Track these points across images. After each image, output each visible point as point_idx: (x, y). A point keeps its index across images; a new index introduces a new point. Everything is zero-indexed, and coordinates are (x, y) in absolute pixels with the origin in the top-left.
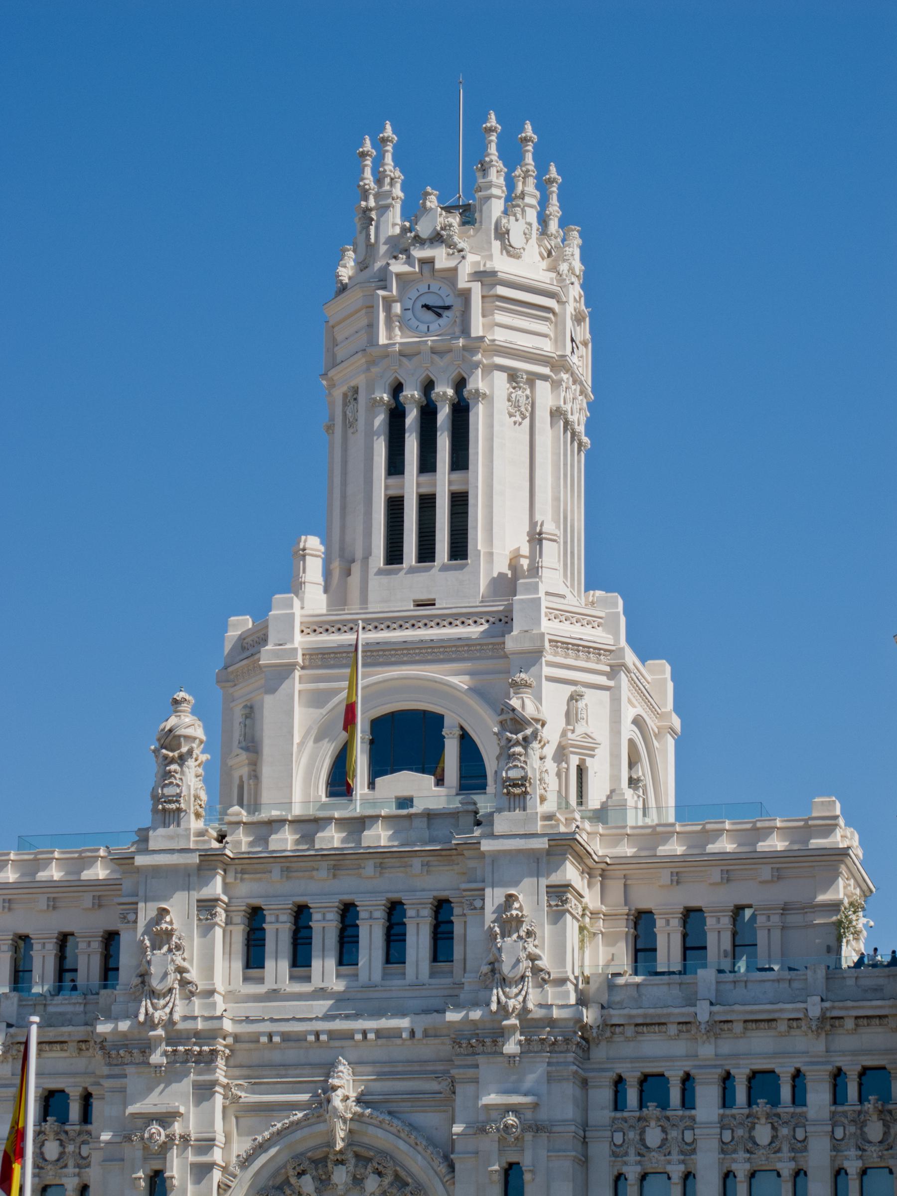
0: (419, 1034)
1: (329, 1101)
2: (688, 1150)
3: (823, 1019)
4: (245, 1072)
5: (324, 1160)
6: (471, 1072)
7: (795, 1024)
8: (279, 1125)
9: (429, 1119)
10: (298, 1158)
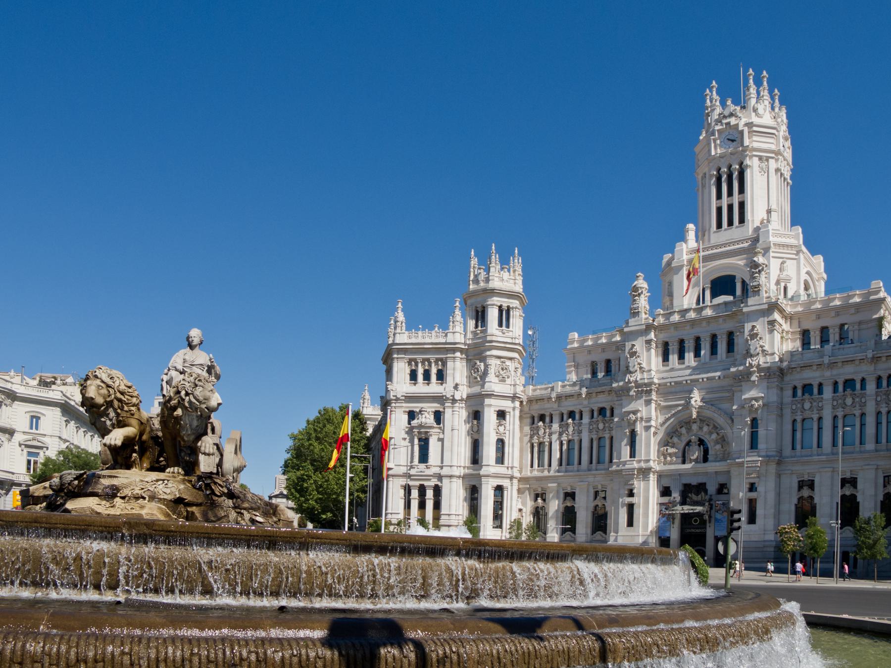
0: (722, 378)
1: (690, 402)
2: (821, 409)
3: (873, 358)
4: (662, 396)
5: (689, 422)
6: (739, 388)
7: (862, 361)
8: (673, 412)
9: (725, 406)
10: (680, 422)
